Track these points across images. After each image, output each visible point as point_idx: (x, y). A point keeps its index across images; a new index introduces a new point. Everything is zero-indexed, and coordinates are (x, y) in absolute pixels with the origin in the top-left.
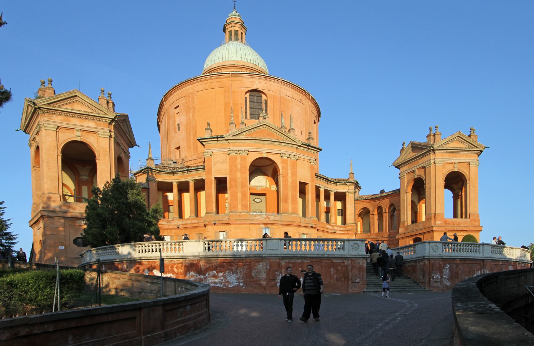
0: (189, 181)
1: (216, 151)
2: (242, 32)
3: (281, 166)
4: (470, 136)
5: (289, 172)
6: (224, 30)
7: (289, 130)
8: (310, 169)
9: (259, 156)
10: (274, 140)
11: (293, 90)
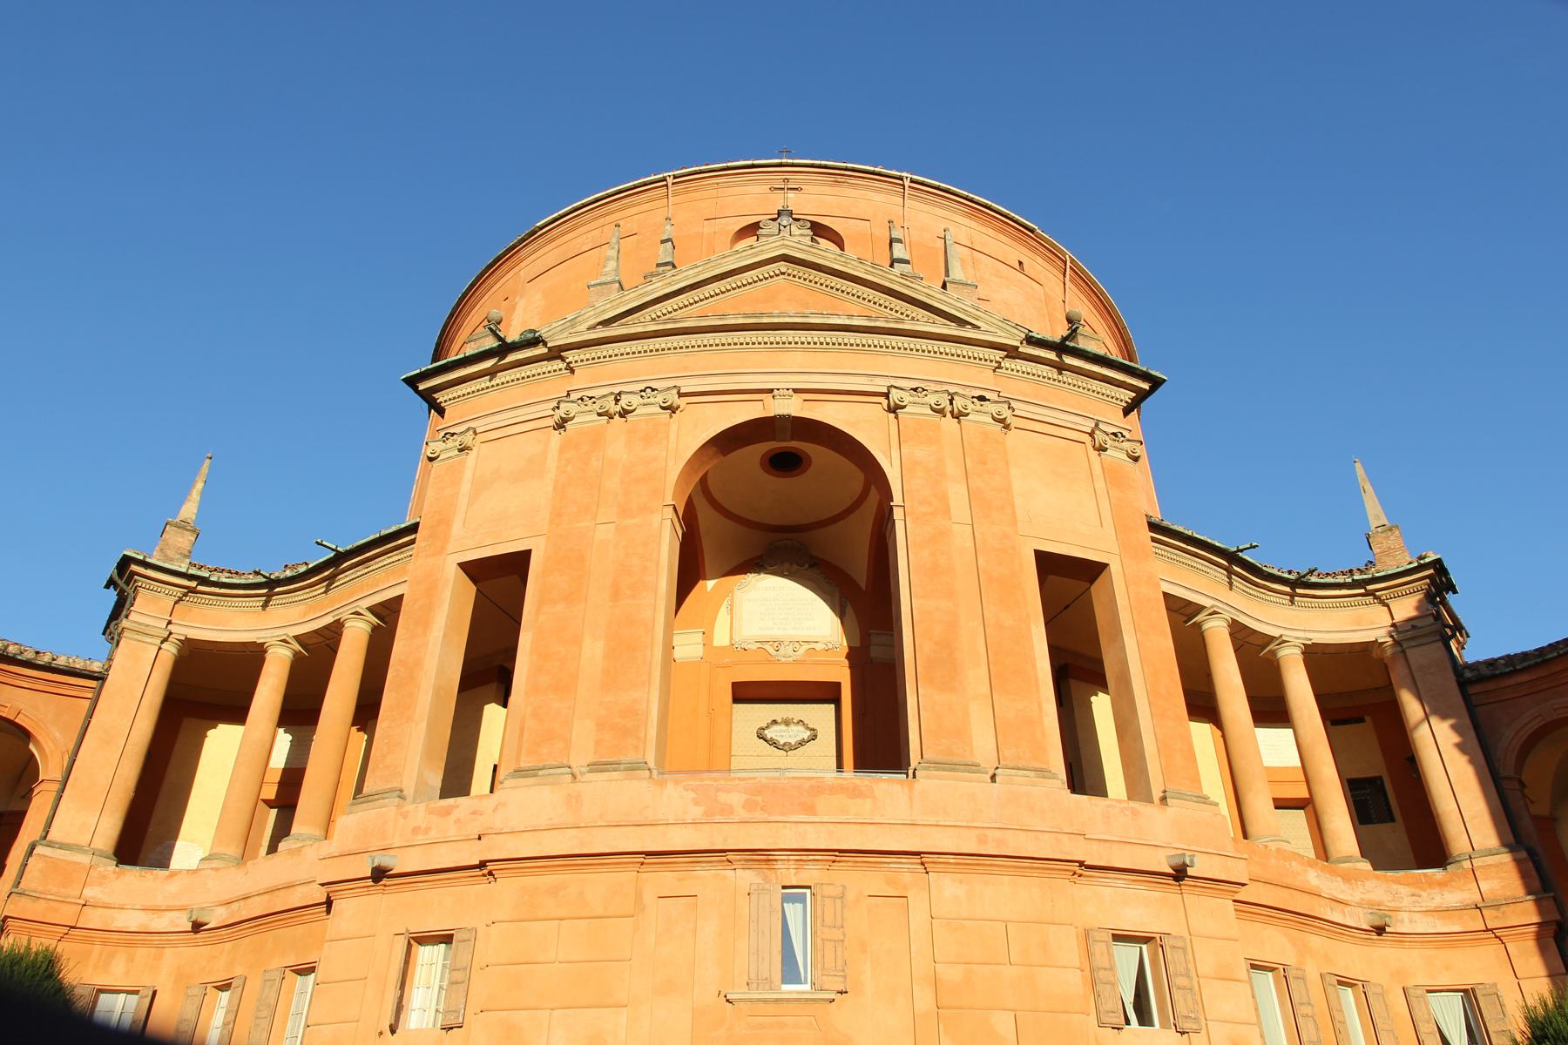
3: (896, 462)
8: (1100, 484)
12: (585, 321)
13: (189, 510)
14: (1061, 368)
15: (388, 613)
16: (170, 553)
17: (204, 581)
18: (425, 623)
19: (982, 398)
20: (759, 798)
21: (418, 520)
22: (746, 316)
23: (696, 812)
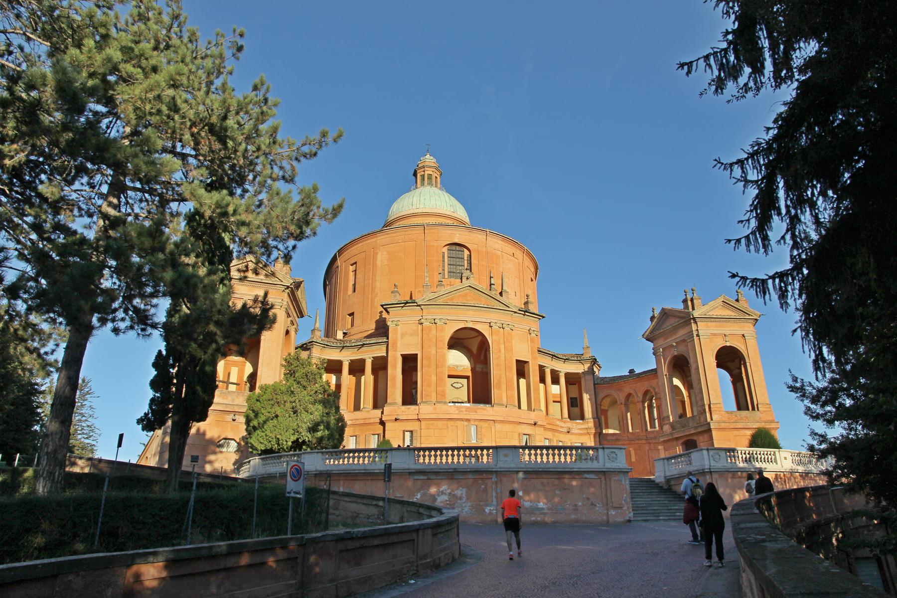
1: (405, 319)
4: (737, 300)
5: (502, 346)
6: (415, 174)
7: (501, 294)
9: (461, 325)
11: (503, 243)
14: (524, 315)
18: (395, 367)
23: (457, 412)
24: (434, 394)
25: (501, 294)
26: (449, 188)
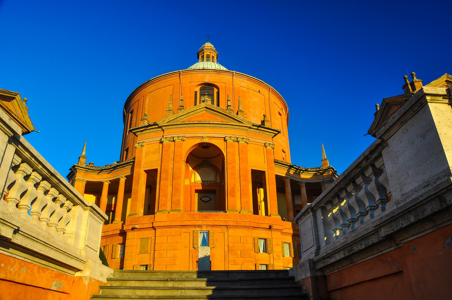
0: (120, 178)
2: (214, 56)
5: (237, 158)
8: (265, 154)
9: (198, 141)
10: (216, 123)
11: (249, 82)
12: (166, 121)
13: (84, 153)
15: (129, 180)
16: (82, 163)
17: (89, 169)
19: (243, 138)
20: (200, 216)
21: (134, 160)
22: (198, 121)
24: (169, 204)
25: (237, 114)
26: (220, 61)
